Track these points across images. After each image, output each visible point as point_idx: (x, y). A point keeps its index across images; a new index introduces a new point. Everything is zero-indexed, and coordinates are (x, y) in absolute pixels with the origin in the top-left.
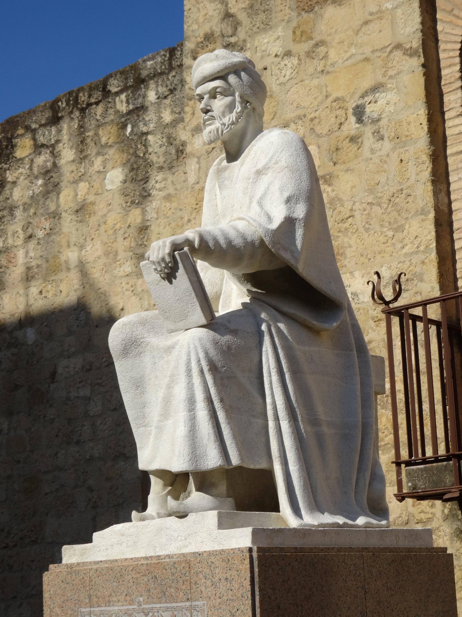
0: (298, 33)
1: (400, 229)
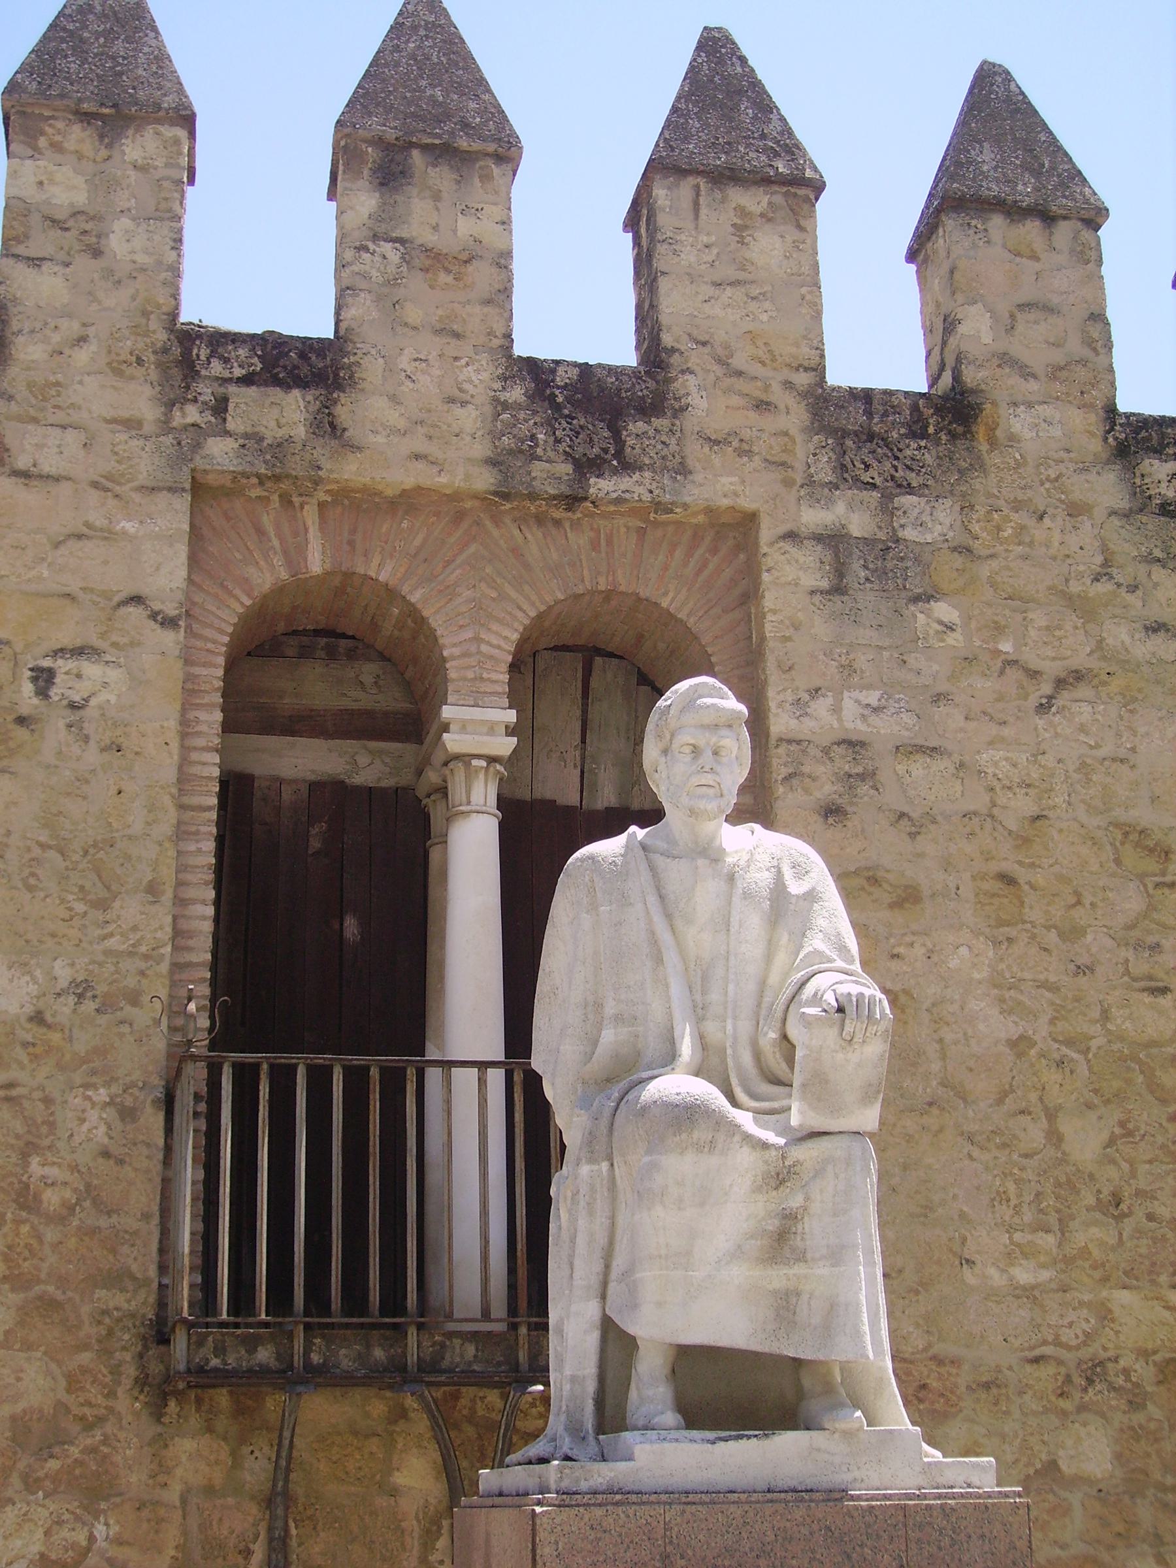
1: (102, 905)
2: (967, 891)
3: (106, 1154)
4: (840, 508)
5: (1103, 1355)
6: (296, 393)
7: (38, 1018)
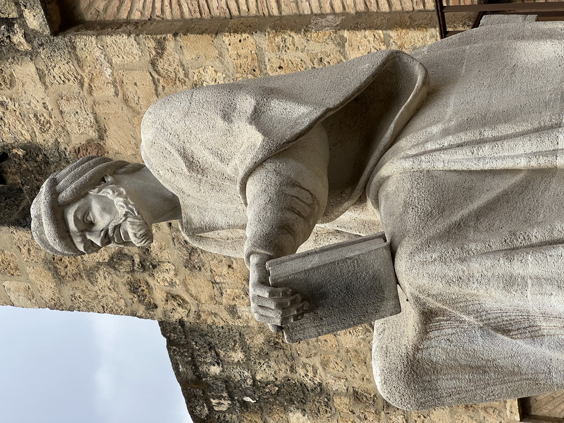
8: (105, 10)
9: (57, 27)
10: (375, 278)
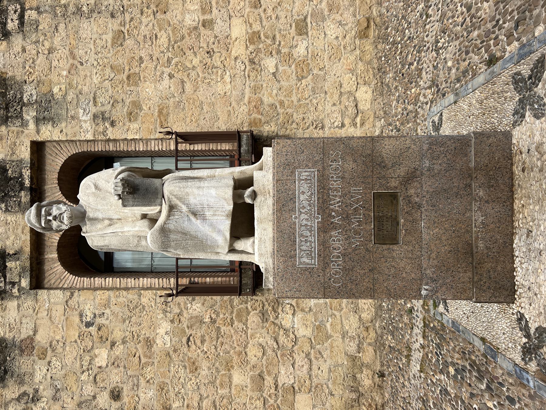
0: (41, 356)
2: (132, 88)
3: (203, 304)
4: (29, 118)
5: (248, 58)
6: (7, 264)
7: (172, 321)
8: (54, 284)
9: (32, 288)
10: (156, 189)
